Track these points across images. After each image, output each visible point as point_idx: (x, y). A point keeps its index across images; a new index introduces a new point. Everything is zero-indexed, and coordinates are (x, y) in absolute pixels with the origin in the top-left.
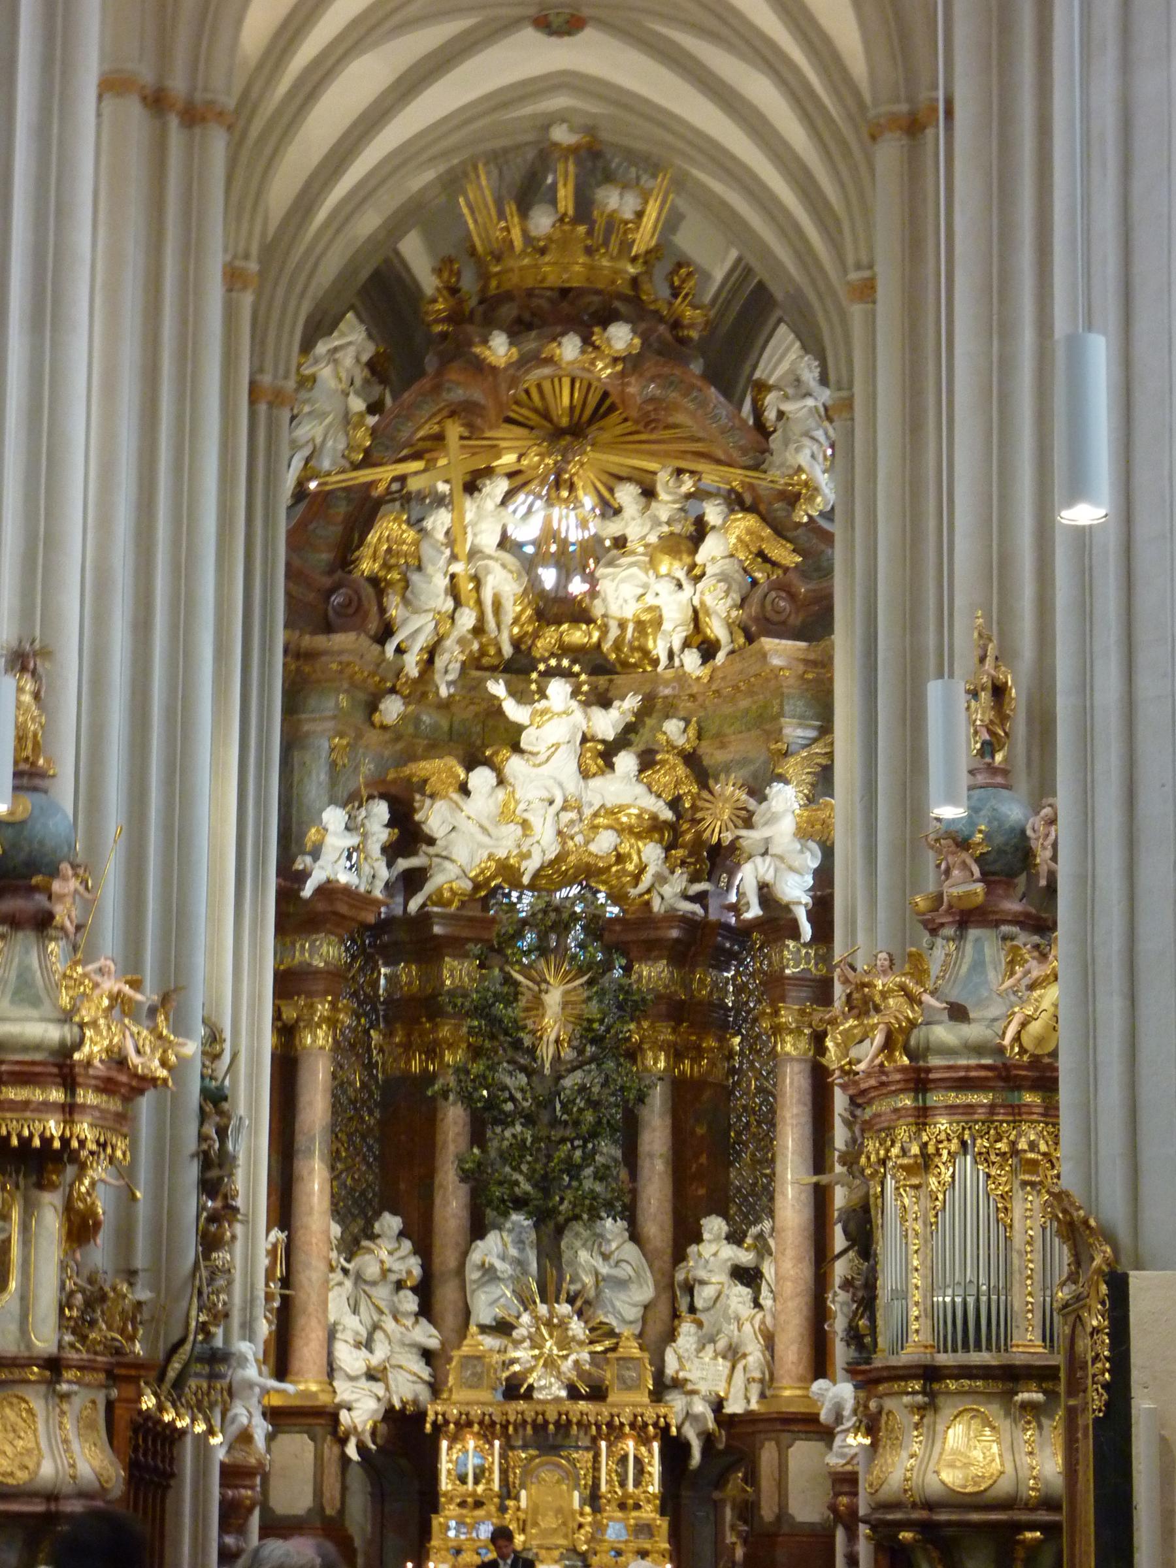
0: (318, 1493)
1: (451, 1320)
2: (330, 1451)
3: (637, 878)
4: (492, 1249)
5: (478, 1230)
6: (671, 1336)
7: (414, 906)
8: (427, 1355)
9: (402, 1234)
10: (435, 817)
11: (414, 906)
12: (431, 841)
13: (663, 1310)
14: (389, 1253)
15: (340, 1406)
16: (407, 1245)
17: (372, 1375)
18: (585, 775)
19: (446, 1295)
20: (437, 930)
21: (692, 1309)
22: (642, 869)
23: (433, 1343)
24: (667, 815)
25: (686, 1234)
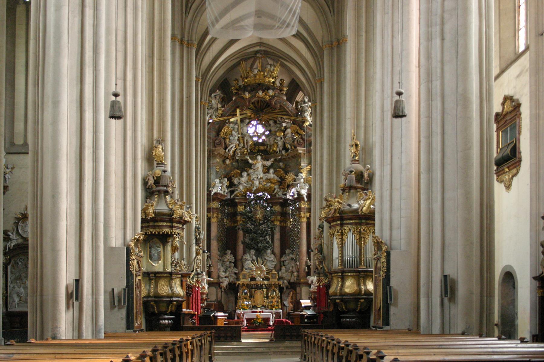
0: (217, 297)
1: (240, 268)
2: (219, 290)
3: (274, 191)
4: (247, 256)
5: (245, 253)
6: (280, 270)
7: (232, 197)
8: (236, 274)
9: (231, 254)
10: (236, 181)
11: (232, 197)
12: (235, 185)
13: (278, 265)
14: (229, 257)
15: (220, 282)
16: (232, 255)
17: (226, 277)
18: (264, 173)
19: (239, 263)
20: (237, 201)
21: (284, 265)
22: (275, 189)
23: (237, 272)
24: (280, 180)
25: (283, 253)
